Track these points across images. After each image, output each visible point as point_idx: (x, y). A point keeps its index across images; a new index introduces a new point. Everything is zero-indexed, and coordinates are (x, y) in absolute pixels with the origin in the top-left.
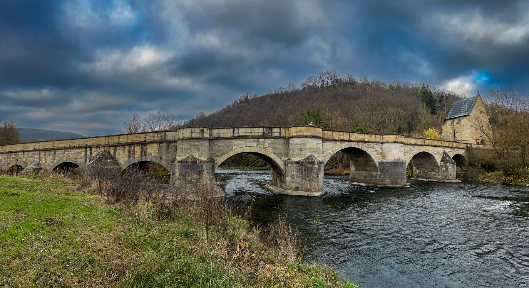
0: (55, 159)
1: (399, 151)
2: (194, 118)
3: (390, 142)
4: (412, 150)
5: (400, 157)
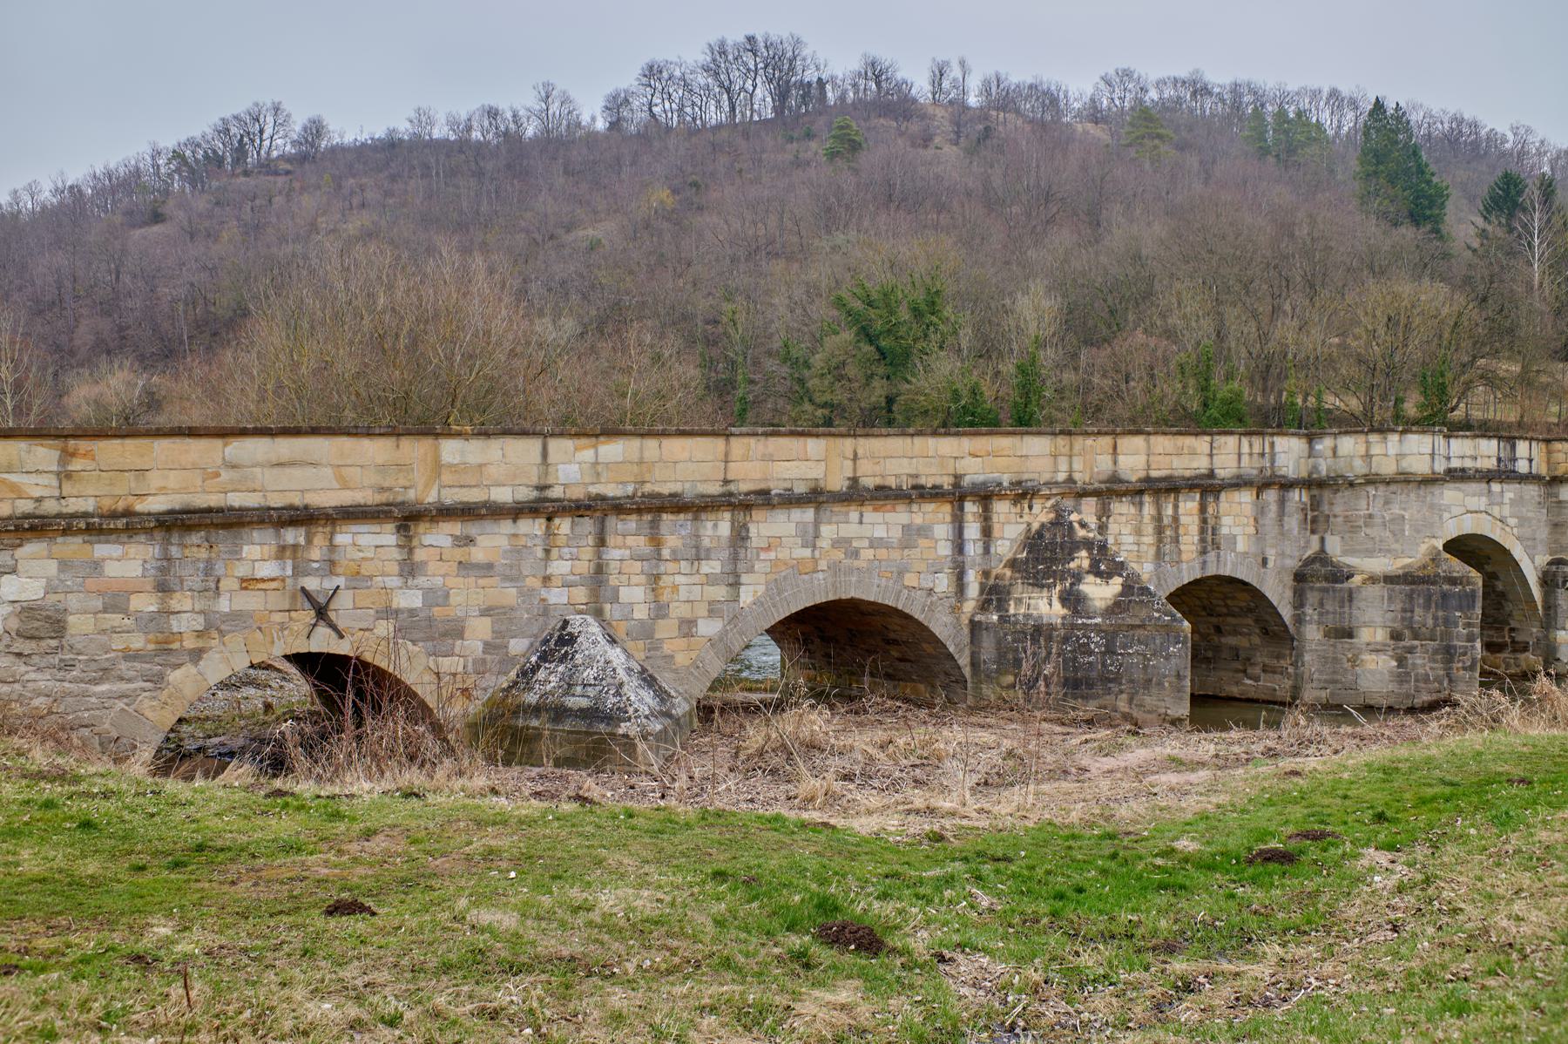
0: (744, 578)
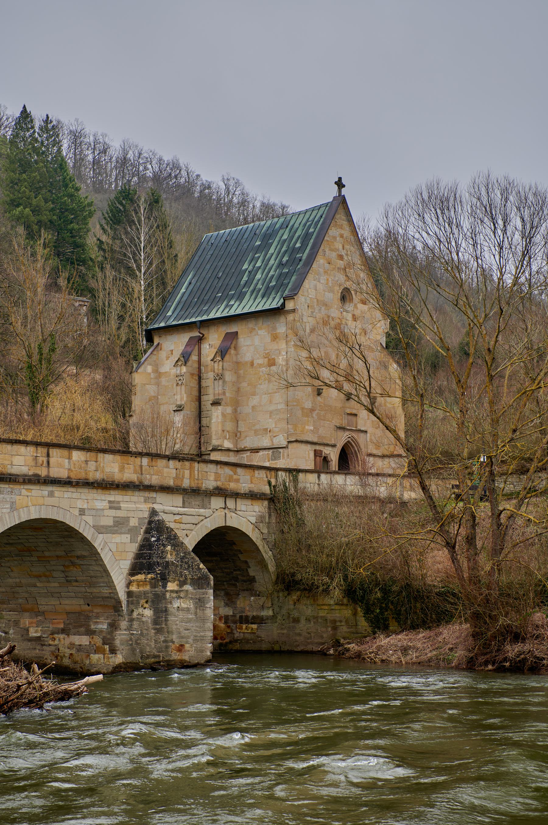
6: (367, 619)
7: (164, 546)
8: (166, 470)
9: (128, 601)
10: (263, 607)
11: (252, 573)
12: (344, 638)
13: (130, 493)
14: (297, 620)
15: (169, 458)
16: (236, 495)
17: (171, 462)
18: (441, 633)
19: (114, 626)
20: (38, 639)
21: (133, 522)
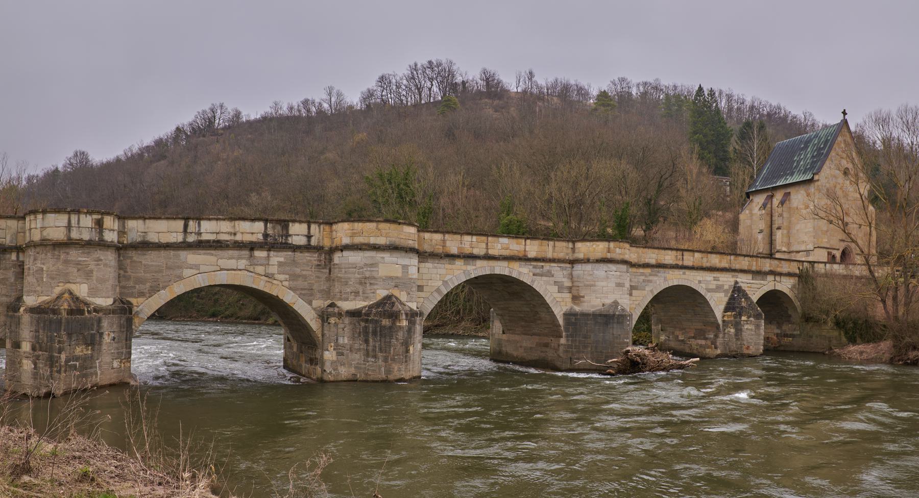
1: (614, 285)
2: (57, 168)
3: (593, 257)
4: (650, 281)
5: (619, 301)
6: (846, 337)
7: (741, 299)
8: (743, 262)
9: (723, 325)
10: (795, 330)
11: (790, 313)
12: (834, 346)
13: (724, 273)
14: (811, 337)
15: (745, 256)
16: (781, 274)
17: (746, 258)
18: (880, 345)
19: (716, 336)
20: (683, 340)
21: (726, 287)
